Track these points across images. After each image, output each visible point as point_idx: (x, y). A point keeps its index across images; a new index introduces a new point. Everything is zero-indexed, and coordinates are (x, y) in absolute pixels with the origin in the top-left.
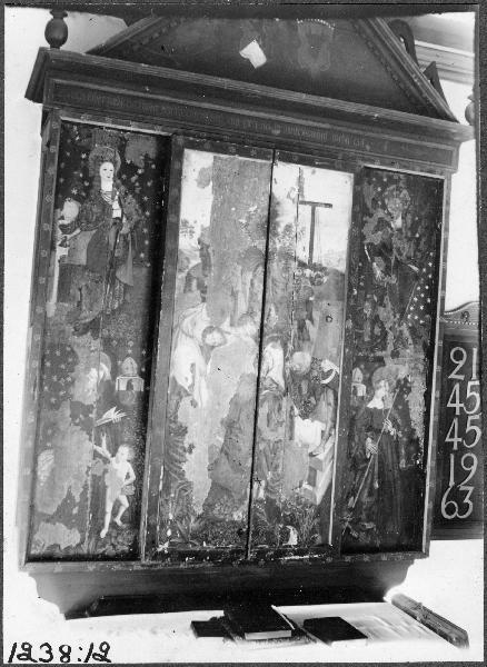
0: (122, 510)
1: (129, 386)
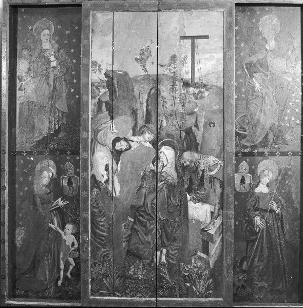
0: (71, 268)
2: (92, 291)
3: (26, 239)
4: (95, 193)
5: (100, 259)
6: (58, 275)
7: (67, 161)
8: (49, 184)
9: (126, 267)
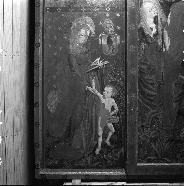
1: (109, 41)
2: (139, 158)
3: (60, 103)
4: (143, 47)
5: (149, 122)
6: (96, 143)
7: (107, 17)
8: (86, 43)
9: (176, 130)
